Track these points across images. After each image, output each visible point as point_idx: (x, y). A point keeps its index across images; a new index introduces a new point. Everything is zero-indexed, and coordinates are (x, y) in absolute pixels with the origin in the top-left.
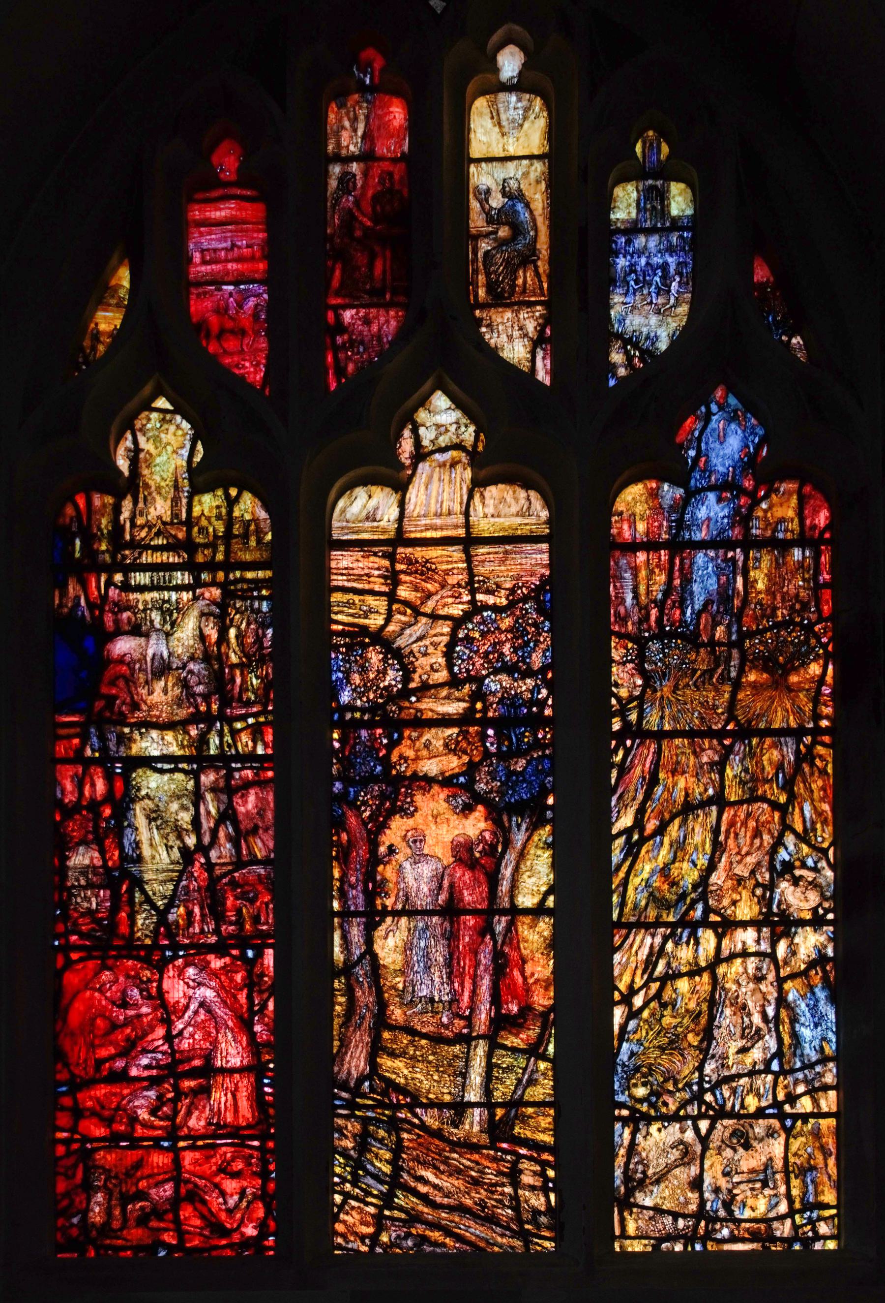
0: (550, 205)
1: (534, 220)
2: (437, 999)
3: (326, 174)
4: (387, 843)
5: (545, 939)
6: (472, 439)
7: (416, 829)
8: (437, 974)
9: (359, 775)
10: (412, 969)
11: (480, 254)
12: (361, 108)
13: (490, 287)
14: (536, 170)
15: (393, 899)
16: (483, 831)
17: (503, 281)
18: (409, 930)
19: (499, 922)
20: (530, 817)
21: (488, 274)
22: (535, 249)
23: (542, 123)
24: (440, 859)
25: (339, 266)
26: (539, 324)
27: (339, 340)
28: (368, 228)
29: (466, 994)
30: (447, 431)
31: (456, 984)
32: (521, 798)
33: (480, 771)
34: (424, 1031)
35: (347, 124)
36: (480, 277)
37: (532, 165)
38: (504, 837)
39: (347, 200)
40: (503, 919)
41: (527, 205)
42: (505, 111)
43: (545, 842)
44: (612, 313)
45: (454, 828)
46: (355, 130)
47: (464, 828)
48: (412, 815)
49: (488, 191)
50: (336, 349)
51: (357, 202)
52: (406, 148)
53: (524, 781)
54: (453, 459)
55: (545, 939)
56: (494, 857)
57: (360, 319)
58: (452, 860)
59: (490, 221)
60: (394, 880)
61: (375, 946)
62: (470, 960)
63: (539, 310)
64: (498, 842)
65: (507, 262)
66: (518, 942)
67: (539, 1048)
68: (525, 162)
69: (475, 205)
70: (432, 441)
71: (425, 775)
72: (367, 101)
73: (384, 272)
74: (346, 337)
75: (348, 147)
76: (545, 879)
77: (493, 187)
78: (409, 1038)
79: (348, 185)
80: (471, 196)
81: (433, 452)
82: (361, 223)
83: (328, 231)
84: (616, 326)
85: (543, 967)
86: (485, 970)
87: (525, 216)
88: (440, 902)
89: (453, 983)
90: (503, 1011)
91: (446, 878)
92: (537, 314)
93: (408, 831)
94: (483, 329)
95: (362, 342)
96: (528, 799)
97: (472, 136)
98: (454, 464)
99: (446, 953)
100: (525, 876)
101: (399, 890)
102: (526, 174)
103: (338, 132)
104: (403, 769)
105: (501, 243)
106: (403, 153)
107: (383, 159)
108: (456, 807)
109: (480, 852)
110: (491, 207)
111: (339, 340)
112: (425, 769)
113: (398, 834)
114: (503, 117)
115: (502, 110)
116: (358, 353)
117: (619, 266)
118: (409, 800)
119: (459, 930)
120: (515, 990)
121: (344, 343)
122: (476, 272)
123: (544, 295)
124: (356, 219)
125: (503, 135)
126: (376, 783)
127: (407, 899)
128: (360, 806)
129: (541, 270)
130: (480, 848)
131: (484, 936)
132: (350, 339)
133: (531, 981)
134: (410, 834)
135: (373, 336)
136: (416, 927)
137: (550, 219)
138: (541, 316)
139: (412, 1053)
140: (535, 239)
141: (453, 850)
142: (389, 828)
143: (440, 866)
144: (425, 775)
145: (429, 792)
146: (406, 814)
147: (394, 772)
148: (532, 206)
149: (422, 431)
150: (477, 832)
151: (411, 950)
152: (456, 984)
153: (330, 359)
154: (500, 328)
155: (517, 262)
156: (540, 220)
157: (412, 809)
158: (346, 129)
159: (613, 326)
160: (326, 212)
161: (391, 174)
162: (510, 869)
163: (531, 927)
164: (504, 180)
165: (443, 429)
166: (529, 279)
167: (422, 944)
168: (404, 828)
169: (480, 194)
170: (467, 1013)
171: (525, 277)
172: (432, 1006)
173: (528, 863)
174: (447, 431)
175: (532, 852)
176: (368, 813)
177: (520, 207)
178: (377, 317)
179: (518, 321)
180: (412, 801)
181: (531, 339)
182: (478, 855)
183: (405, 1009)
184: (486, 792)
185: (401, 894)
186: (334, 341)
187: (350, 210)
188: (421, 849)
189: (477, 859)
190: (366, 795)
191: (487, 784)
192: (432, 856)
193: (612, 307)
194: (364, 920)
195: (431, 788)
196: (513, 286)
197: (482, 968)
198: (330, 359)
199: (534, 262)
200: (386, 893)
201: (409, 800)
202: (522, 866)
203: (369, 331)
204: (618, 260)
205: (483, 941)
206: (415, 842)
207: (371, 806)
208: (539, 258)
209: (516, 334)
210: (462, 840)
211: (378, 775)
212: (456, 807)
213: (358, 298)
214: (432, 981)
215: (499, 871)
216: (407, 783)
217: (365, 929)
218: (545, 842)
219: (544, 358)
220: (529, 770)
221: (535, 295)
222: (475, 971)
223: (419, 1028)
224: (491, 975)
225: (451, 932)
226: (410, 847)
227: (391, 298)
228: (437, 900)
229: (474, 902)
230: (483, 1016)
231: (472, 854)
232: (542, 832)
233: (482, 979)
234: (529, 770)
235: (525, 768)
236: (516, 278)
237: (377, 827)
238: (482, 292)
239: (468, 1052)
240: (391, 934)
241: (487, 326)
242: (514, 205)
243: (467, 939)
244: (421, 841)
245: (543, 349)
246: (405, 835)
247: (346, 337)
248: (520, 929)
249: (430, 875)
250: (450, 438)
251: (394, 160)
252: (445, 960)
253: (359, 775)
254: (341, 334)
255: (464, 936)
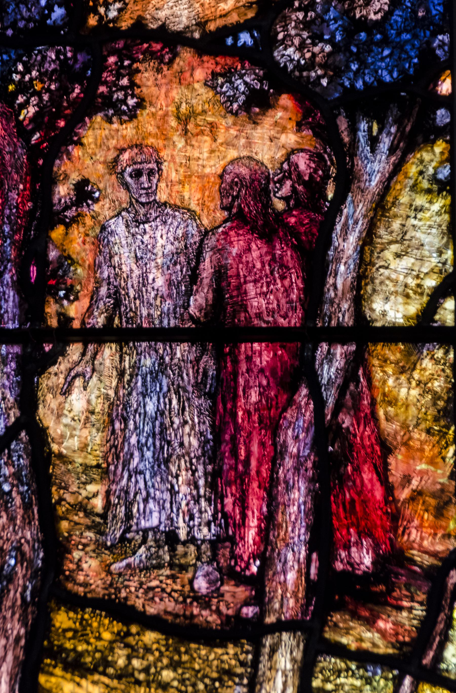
2: (182, 534)
4: (75, 177)
5: (436, 397)
7: (139, 146)
8: (184, 476)
9: (14, 25)
10: (126, 463)
15: (85, 302)
16: (293, 152)
18: (121, 374)
19: (330, 358)
20: (399, 122)
24: (193, 215)
29: (253, 522)
31: (229, 501)
32: (380, 80)
33: (286, 20)
34: (151, 610)
38: (341, 165)
40: (339, 350)
43: (434, 179)
45: (228, 144)
47: (249, 144)
48: (133, 116)
53: (385, 42)
55: (436, 397)
56: (318, 209)
58: (220, 215)
60: (89, 260)
61: (41, 410)
62: (262, 444)
64: (326, 177)
66: (373, 403)
67: (423, 654)
71: (163, 27)
76: (435, 260)
78: (117, 627)
85: (431, 462)
86: (297, 469)
88: (192, 310)
89: (222, 497)
90: (339, 566)
91: (207, 256)
93: (122, 151)
96: (394, 84)
99: (206, 428)
100: (388, 254)
101: (98, 283)
104: (113, 14)
108: (233, 99)
109: (286, 199)
112: (162, 14)
113: (100, 156)
118: (125, 82)
119: (235, 374)
120: (366, 515)
126: (51, 45)
127: (118, 304)
128: (14, 95)
130: (286, 189)
131: (295, 390)
133: (404, 494)
134: (126, 156)
136: (136, 367)
139: (121, 662)
141: (223, 193)
142: (79, 143)
143: (193, 230)
144: (163, 27)
145: (171, 63)
146: (119, 113)
147: (92, 21)
150: (280, 155)
151: (125, 420)
152: (229, 501)
157: (131, 102)
162: (353, 238)
163: (402, 371)
167: (151, 407)
168: (113, 143)
170: (254, 569)
172: (172, 550)
173: (396, 225)
175: (404, 199)
176: (32, 110)
180: (133, 85)
182: (280, 205)
183: (109, 558)
184: (298, 67)
185: (103, 291)
188: (150, 192)
189: (279, 215)
190: (28, 70)
191: (301, 48)
192: (176, 208)
194: (16, 349)
195: (175, 55)
197: (289, 463)
200: (70, 290)
201: (125, 82)
202: (382, 231)
205: (291, 402)
206: (137, 174)
207: (39, 94)
210: (244, 171)
211: (55, 28)
212: (232, 99)
214: (173, 492)
215: (328, 242)
216: (120, 44)
217: (18, 372)
218: (434, 179)
220: (397, 17)
222: (273, 470)
223: (139, 603)
224: (311, 480)
225: (217, 378)
226: (127, 187)
228: (186, 306)
229: (271, 312)
230: (291, 576)
231: (268, 204)
232: (426, 156)
233: (289, 489)
234: (397, 17)
235: (388, 15)
237: (51, 140)
239: (255, 663)
240: (78, 382)
243: (254, 397)
244: (151, 173)
246: (116, 160)
248: (378, 375)
249: (169, 247)
252: (203, 444)
253: (14, 25)
255: (247, 387)
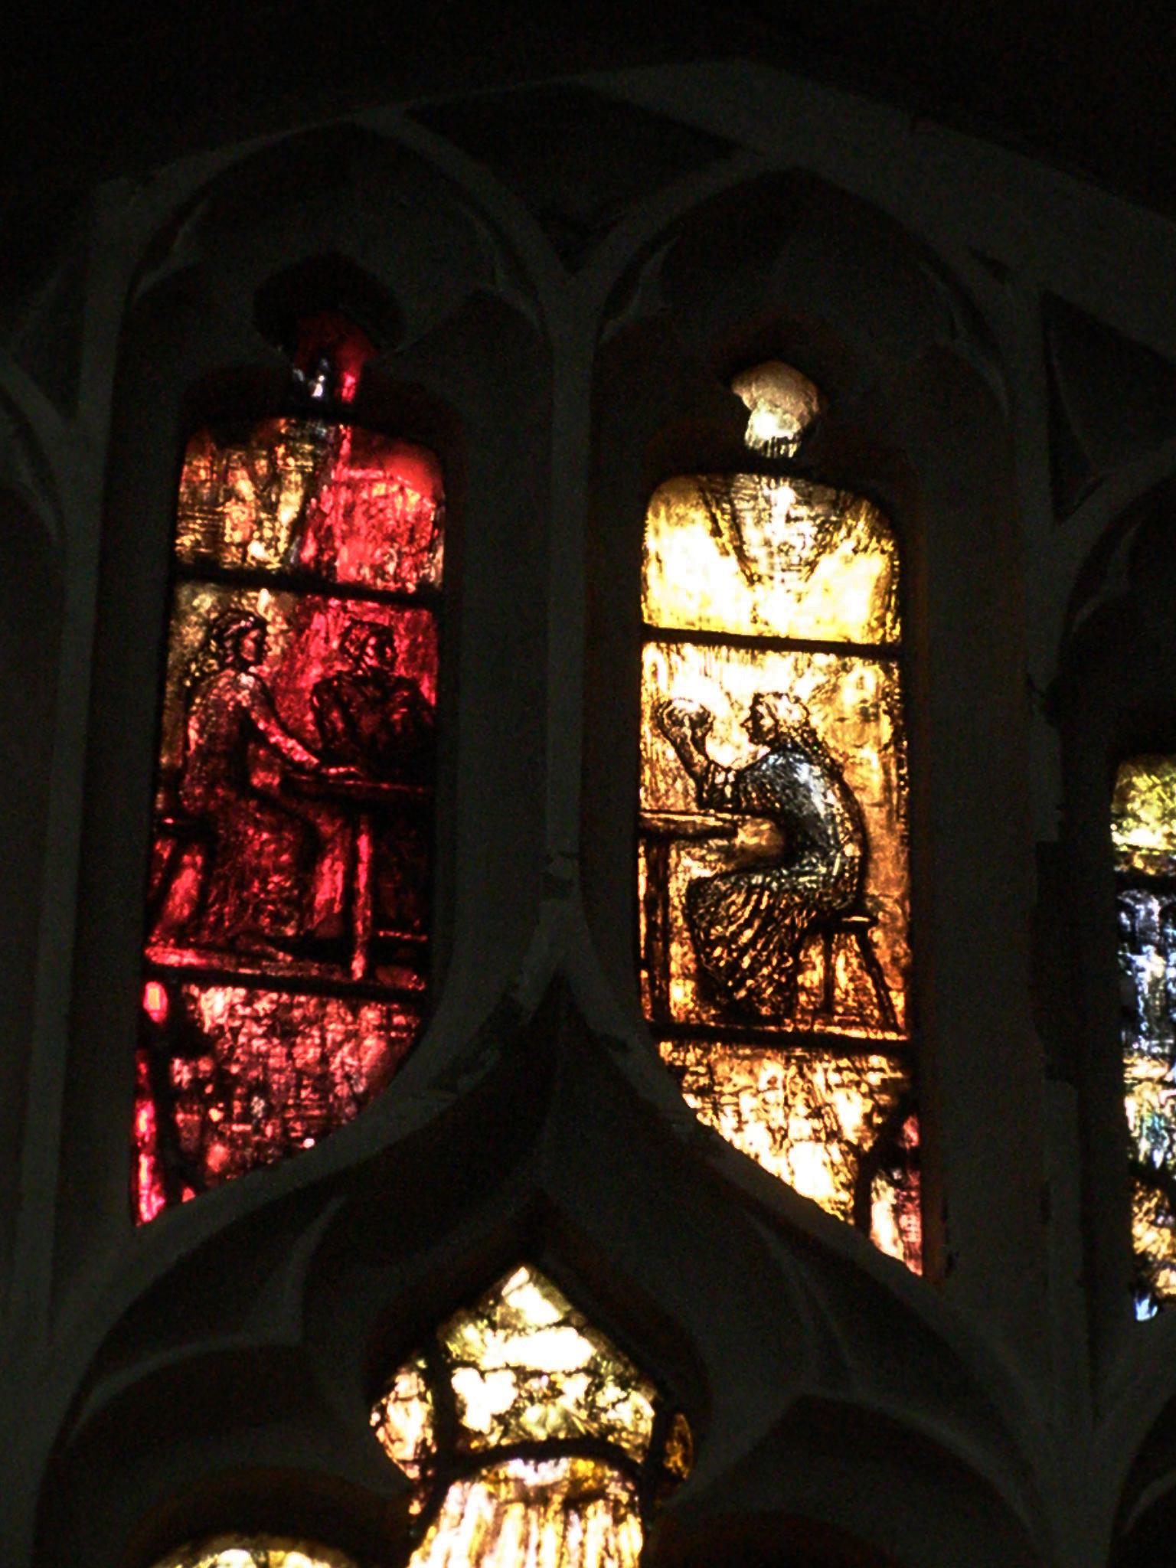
0: (911, 781)
1: (857, 815)
3: (171, 612)
6: (646, 1427)
11: (677, 886)
12: (291, 452)
13: (707, 983)
14: (861, 684)
17: (753, 971)
21: (701, 946)
22: (861, 893)
23: (875, 564)
25: (193, 861)
26: (878, 1109)
27: (182, 1072)
28: (300, 766)
30: (554, 1392)
35: (245, 487)
36: (675, 949)
37: (846, 669)
39: (237, 686)
41: (834, 773)
42: (759, 521)
44: (1131, 1104)
46: (272, 508)
49: (703, 721)
50: (167, 1099)
51: (266, 695)
52: (433, 574)
54: (575, 1482)
57: (257, 1019)
59: (709, 798)
63: (879, 1069)
65: (767, 920)
68: (821, 659)
69: (657, 748)
70: (500, 1419)
72: (314, 439)
73: (349, 894)
74: (205, 1066)
75: (244, 545)
77: (720, 711)
79: (238, 647)
80: (646, 727)
81: (501, 1455)
82: (276, 749)
83: (164, 760)
84: (1144, 1146)
87: (822, 799)
92: (874, 1079)
94: (692, 1101)
95: (262, 1088)
97: (651, 570)
98: (577, 1500)
102: (829, 693)
103: (214, 502)
105: (743, 863)
106: (423, 584)
107: (358, 591)
110: (711, 762)
111: (182, 1072)
114: (751, 534)
115: (748, 519)
116: (246, 1116)
117: (1145, 978)
121: (197, 1083)
122: (663, 933)
123: (895, 1028)
124: (262, 738)
125: (751, 580)
129: (883, 956)
132: (220, 1075)
135: (300, 1073)
137: (909, 819)
138: (886, 1086)
140: (863, 868)
148: (846, 776)
149: (462, 1381)
153: (144, 1121)
154: (747, 1102)
155: (801, 922)
156: (875, 817)
158: (241, 500)
159: (1133, 1144)
160: (160, 710)
161: (385, 636)
164: (757, 699)
165: (536, 1385)
166: (842, 978)
169: (680, 723)
171: (830, 969)
174: (554, 1392)
177: (805, 773)
178: (318, 1021)
179: (810, 1092)
181: (854, 1149)
186: (161, 1072)
187: (242, 714)
193: (1126, 1090)
196: (789, 989)
198: (144, 1121)
199: (861, 931)
203: (290, 1056)
204: (1140, 960)
208: (874, 922)
209: (801, 1126)
213: (254, 960)
219: (897, 1210)
221: (864, 1024)
227: (369, 971)
236: (799, 968)
238: (681, 994)
241: (702, 1092)
242: (790, 768)
245: (892, 1183)
247: (205, 1066)
250: (566, 1416)
251: (397, 600)
254: (190, 1056)
